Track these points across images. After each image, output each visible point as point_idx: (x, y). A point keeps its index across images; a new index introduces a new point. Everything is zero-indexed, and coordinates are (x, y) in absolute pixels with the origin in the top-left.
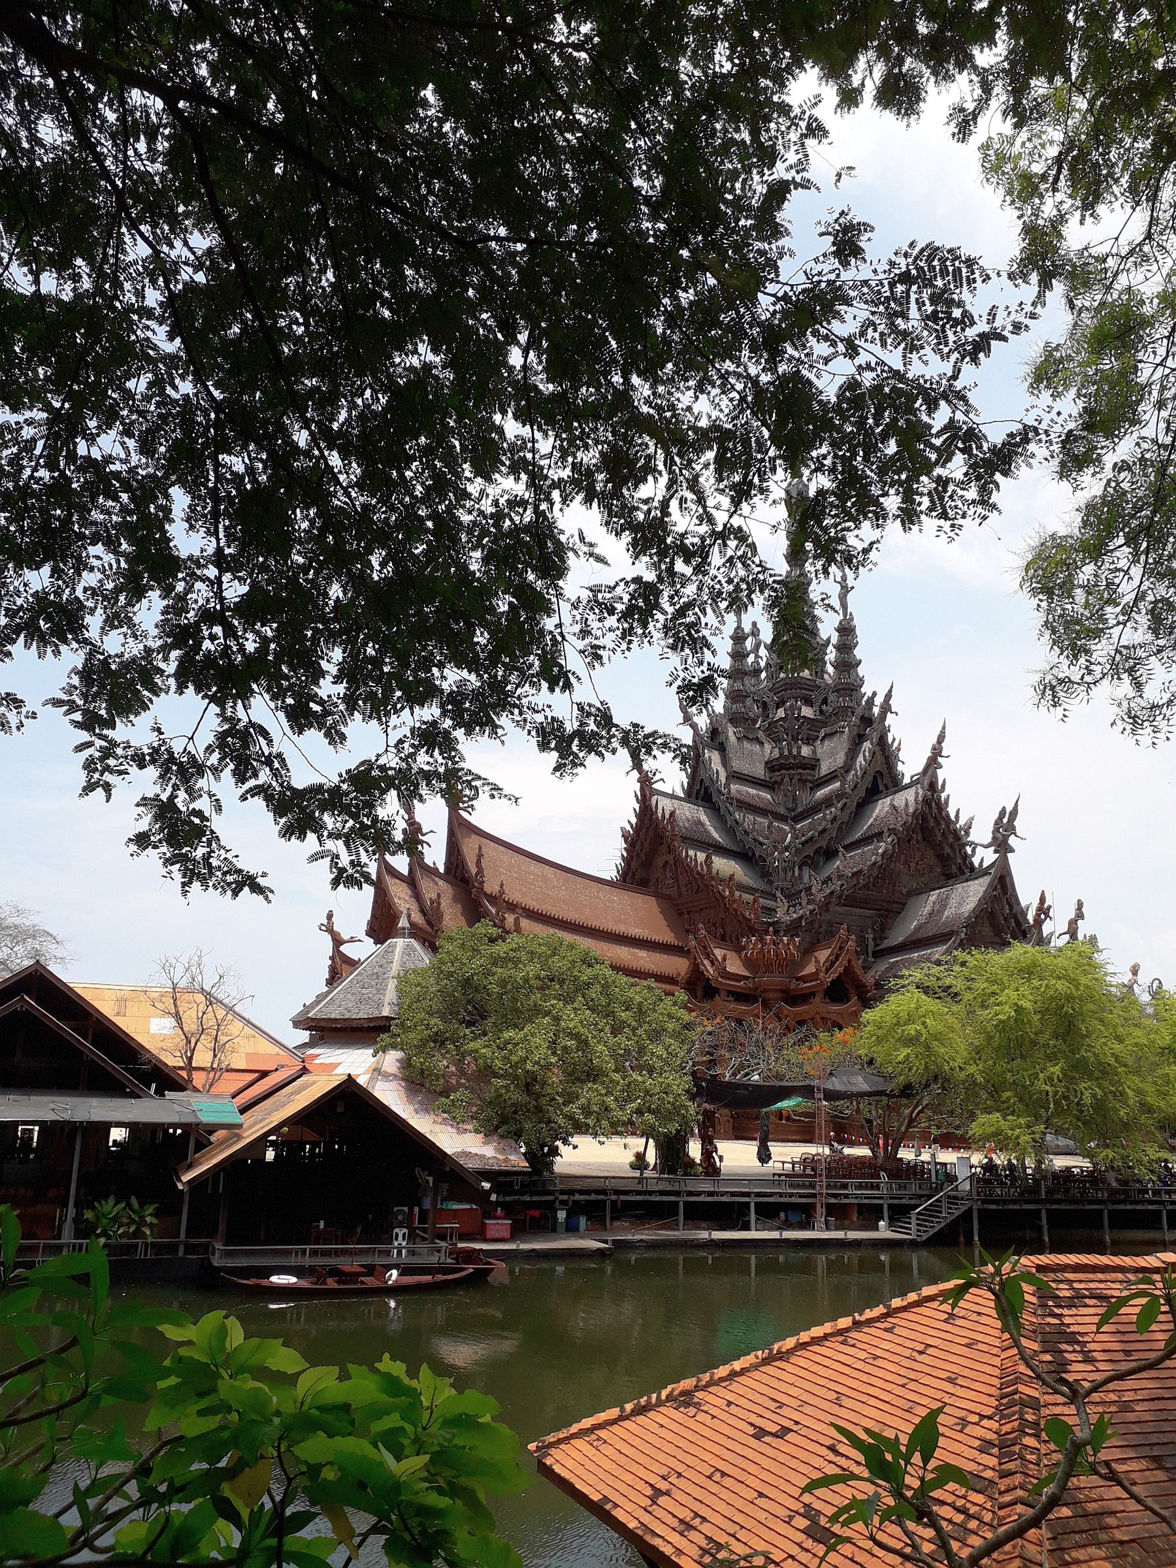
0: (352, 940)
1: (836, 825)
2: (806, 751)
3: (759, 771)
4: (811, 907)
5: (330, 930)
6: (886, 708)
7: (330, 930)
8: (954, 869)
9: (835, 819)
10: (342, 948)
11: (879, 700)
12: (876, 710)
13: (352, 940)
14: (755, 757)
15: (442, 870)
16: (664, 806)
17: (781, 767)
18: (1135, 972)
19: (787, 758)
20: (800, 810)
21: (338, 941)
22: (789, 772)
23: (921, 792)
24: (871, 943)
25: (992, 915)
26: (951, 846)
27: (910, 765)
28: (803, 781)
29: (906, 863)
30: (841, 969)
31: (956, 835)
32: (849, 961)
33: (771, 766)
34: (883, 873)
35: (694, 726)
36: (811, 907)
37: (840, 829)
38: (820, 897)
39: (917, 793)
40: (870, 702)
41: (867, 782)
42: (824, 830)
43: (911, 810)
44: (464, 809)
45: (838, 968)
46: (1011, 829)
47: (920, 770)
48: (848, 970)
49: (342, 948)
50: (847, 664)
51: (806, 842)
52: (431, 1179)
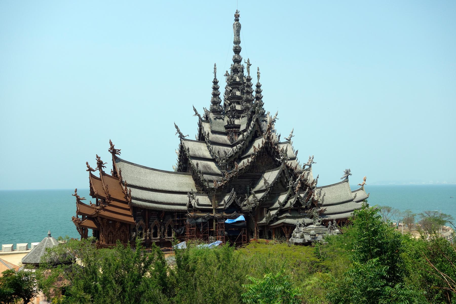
1: (241, 150)
9: (240, 149)
15: (111, 175)
16: (187, 145)
17: (230, 128)
18: (365, 180)
19: (230, 125)
22: (232, 129)
24: (248, 190)
25: (281, 182)
28: (235, 132)
29: (262, 162)
32: (234, 200)
33: (226, 127)
34: (252, 166)
39: (263, 141)
41: (253, 133)
42: (237, 152)
43: (261, 146)
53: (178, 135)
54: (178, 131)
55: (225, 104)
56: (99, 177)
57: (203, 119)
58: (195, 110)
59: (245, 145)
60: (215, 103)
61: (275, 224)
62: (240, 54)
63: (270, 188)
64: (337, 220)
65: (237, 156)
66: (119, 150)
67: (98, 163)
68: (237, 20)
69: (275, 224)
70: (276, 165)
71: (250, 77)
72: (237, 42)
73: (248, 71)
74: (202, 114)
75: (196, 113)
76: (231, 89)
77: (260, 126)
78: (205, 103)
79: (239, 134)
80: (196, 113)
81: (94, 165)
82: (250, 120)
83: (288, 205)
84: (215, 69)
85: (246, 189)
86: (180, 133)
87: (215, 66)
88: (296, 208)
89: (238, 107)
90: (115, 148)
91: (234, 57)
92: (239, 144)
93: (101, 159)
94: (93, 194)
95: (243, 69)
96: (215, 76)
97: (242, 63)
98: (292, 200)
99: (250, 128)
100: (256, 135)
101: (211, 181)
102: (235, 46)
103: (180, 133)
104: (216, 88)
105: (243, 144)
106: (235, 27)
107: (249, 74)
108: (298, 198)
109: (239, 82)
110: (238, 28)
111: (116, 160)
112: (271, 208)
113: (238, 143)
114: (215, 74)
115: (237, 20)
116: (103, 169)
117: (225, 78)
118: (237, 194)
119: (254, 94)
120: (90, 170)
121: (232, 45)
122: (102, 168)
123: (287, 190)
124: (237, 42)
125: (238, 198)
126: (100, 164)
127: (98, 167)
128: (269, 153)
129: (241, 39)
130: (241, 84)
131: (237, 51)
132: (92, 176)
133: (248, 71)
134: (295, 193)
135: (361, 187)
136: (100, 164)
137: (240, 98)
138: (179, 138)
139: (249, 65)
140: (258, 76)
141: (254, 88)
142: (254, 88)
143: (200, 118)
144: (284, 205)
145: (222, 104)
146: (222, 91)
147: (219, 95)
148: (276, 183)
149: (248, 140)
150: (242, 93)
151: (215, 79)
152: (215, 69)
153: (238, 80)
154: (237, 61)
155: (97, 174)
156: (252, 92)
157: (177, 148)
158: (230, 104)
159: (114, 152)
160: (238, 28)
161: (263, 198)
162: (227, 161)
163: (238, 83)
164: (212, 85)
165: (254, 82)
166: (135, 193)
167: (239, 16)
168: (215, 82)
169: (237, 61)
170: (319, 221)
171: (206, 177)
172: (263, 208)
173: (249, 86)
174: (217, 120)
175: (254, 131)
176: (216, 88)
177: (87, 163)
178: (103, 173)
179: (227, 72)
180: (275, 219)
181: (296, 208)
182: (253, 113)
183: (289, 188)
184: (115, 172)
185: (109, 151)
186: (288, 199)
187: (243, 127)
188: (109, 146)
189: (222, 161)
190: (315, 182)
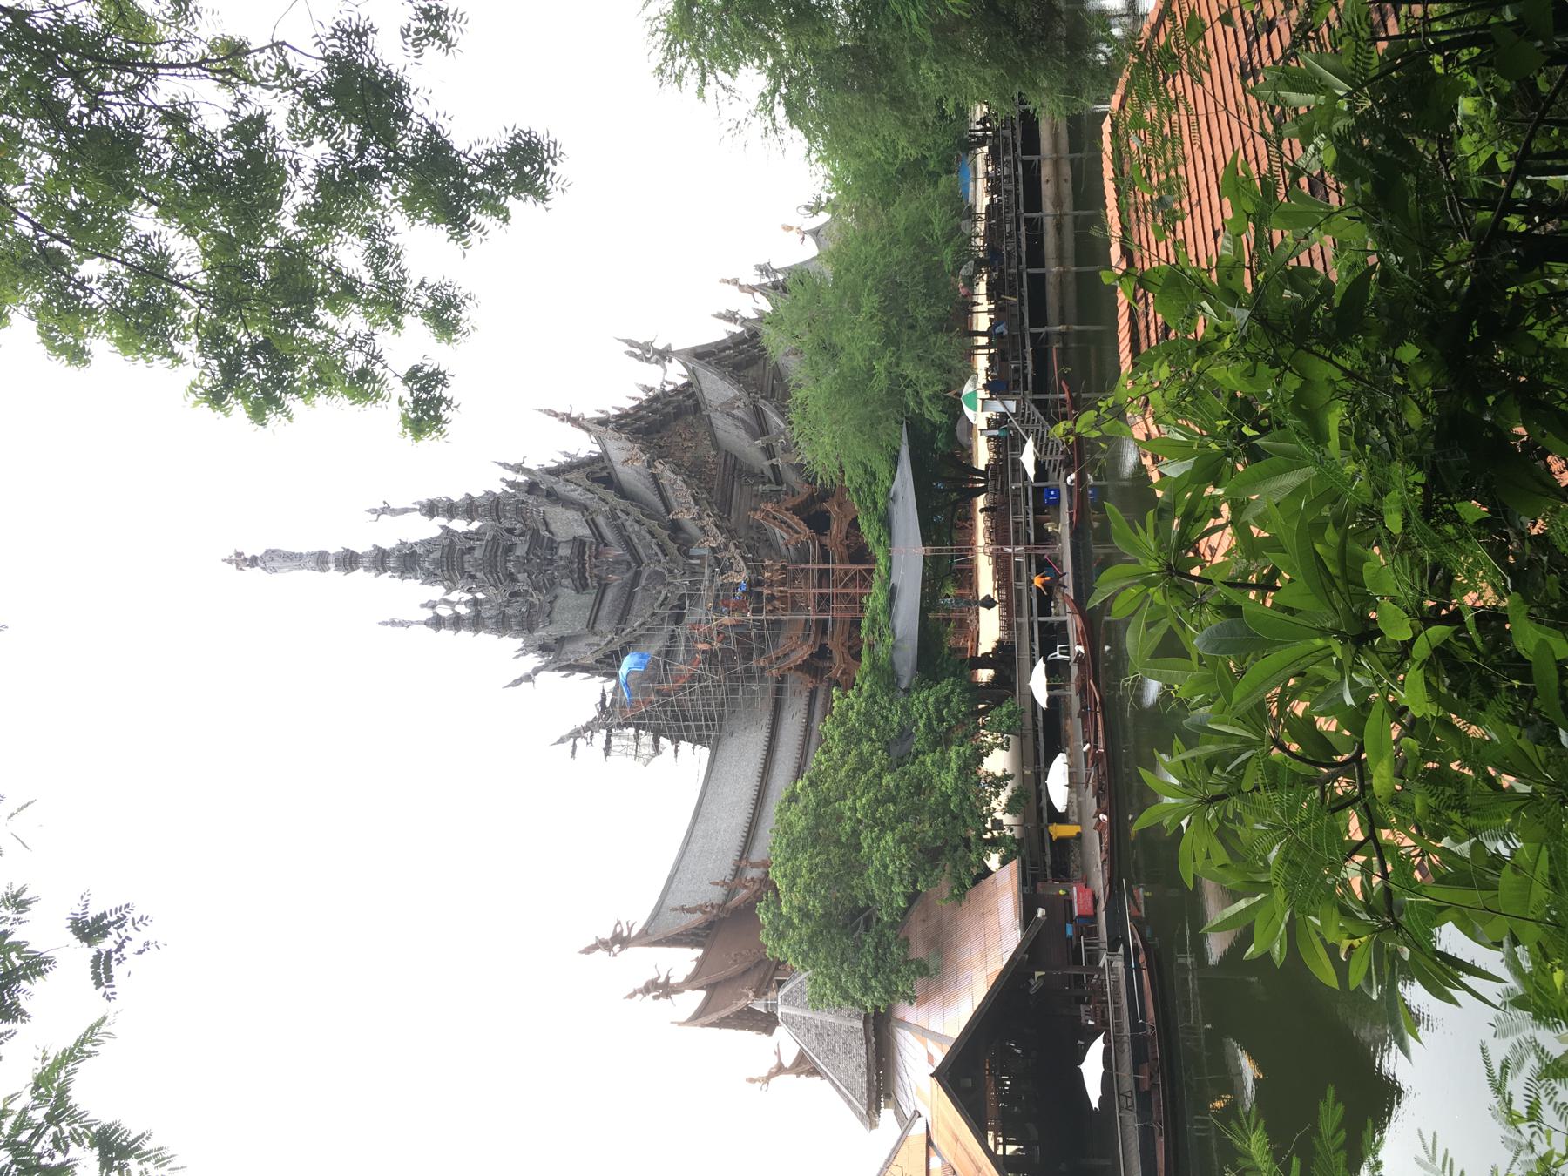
0: (778, 1053)
2: (564, 551)
3: (588, 599)
4: (732, 548)
6: (518, 468)
8: (690, 402)
9: (638, 522)
10: (787, 1064)
11: (511, 476)
12: (521, 478)
13: (778, 1053)
14: (571, 606)
15: (699, 952)
17: (582, 577)
18: (789, 228)
19: (572, 571)
20: (628, 557)
21: (780, 1069)
24: (767, 487)
26: (667, 404)
27: (583, 445)
29: (684, 450)
30: (796, 518)
31: (656, 399)
33: (582, 587)
34: (694, 473)
35: (536, 671)
36: (732, 548)
37: (648, 516)
38: (721, 539)
40: (512, 484)
42: (651, 533)
44: (630, 929)
45: (795, 521)
46: (646, 347)
47: (584, 434)
48: (796, 510)
49: (787, 1064)
50: (469, 508)
51: (663, 551)
52: (1037, 974)
59: (631, 509)
62: (359, 549)
68: (253, 562)
72: (321, 560)
74: (533, 660)
75: (528, 678)
78: (503, 652)
80: (528, 678)
84: (393, 623)
87: (385, 623)
89: (521, 551)
90: (608, 936)
91: (367, 569)
93: (641, 985)
96: (418, 623)
99: (575, 495)
102: (332, 566)
106: (275, 564)
110: (275, 560)
115: (253, 562)
116: (678, 978)
121: (334, 576)
124: (321, 560)
126: (662, 988)
129: (315, 548)
131: (348, 561)
135: (809, 238)
136: (662, 988)
152: (393, 623)
153: (436, 555)
154: (380, 560)
159: (620, 941)
160: (275, 560)
164: (446, 634)
167: (239, 555)
174: (555, 615)
175: (588, 483)
178: (692, 982)
188: (600, 954)
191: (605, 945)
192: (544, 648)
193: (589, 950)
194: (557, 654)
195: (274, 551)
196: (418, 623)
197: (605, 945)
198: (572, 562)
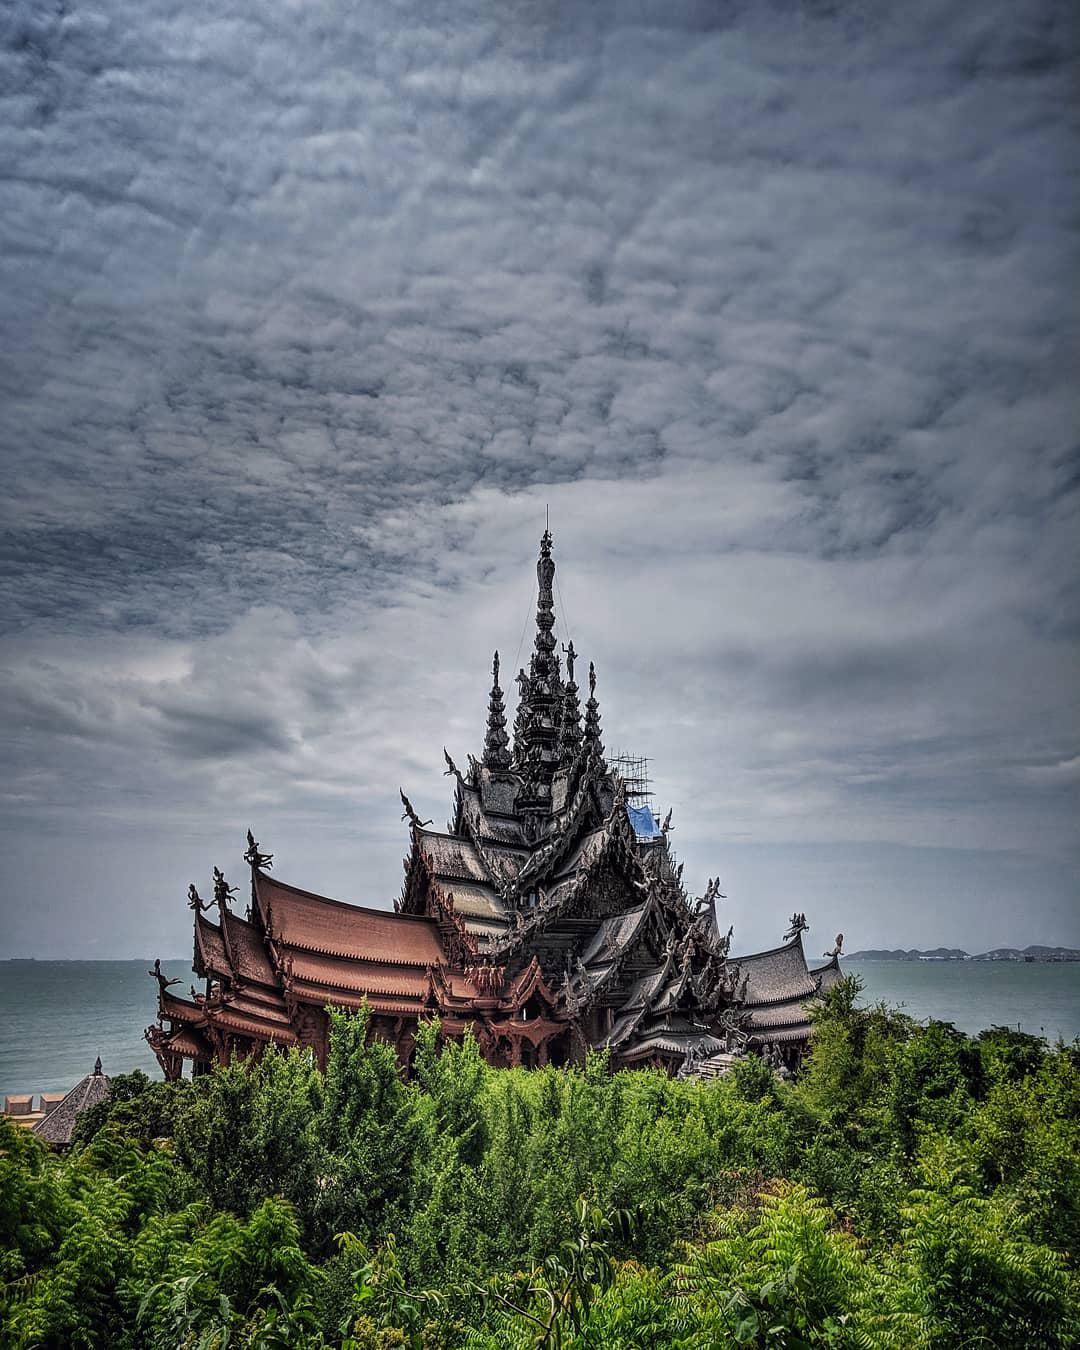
3: (509, 808)
5: (158, 975)
7: (158, 975)
9: (551, 857)
14: (506, 796)
21: (164, 983)
23: (607, 836)
25: (647, 942)
32: (537, 987)
33: (518, 803)
34: (581, 901)
35: (458, 773)
39: (603, 838)
45: (529, 993)
53: (409, 820)
54: (409, 810)
55: (516, 748)
56: (218, 925)
57: (466, 782)
58: (449, 760)
60: (495, 744)
61: (633, 1051)
63: (622, 956)
64: (781, 1043)
65: (544, 876)
66: (269, 857)
67: (216, 889)
69: (633, 1051)
70: (636, 899)
71: (574, 684)
72: (546, 602)
73: (571, 670)
74: (465, 768)
75: (452, 768)
76: (530, 711)
77: (595, 799)
78: (471, 747)
79: (550, 820)
80: (452, 768)
81: (208, 896)
82: (573, 788)
83: (666, 1001)
85: (564, 958)
86: (413, 816)
87: (496, 656)
88: (684, 1009)
91: (538, 636)
92: (549, 844)
94: (200, 967)
95: (557, 663)
96: (496, 681)
97: (555, 653)
98: (675, 990)
100: (588, 823)
101: (484, 938)
103: (413, 816)
104: (496, 709)
105: (559, 845)
107: (572, 678)
108: (688, 984)
109: (550, 695)
111: (259, 879)
112: (624, 1008)
113: (546, 842)
114: (496, 677)
117: (518, 686)
118: (544, 970)
119: (582, 724)
120: (197, 904)
122: (227, 900)
123: (661, 963)
124: (546, 602)
125: (545, 982)
126: (222, 892)
127: (217, 897)
128: (618, 869)
130: (552, 701)
131: (545, 622)
132: (202, 923)
133: (571, 670)
134: (680, 973)
136: (222, 892)
137: (552, 734)
138: (411, 829)
139: (572, 656)
140: (593, 683)
141: (583, 710)
142: (583, 710)
143: (460, 781)
144: (655, 1002)
145: (510, 747)
146: (511, 715)
147: (504, 724)
148: (634, 945)
149: (569, 836)
150: (557, 722)
151: (496, 687)
152: (496, 663)
154: (545, 645)
155: (213, 916)
156: (579, 720)
157: (406, 852)
158: (527, 749)
159: (256, 860)
161: (605, 982)
162: (521, 886)
163: (549, 699)
165: (583, 696)
166: (302, 968)
167: (550, 544)
168: (497, 694)
169: (545, 645)
170: (740, 1046)
171: (472, 928)
172: (607, 1008)
173: (573, 705)
174: (498, 784)
176: (496, 709)
177: (192, 888)
178: (226, 915)
179: (522, 671)
180: (634, 1038)
181: (684, 1009)
182: (581, 769)
183: (666, 957)
184: (255, 913)
185: (246, 858)
186: (665, 985)
187: (558, 803)
189: (509, 887)
190: (724, 944)
191: (253, 850)
192: (475, 778)
193: (250, 839)
194: (471, 787)
195: (553, 570)
196: (496, 681)
197: (253, 850)
198: (534, 797)
